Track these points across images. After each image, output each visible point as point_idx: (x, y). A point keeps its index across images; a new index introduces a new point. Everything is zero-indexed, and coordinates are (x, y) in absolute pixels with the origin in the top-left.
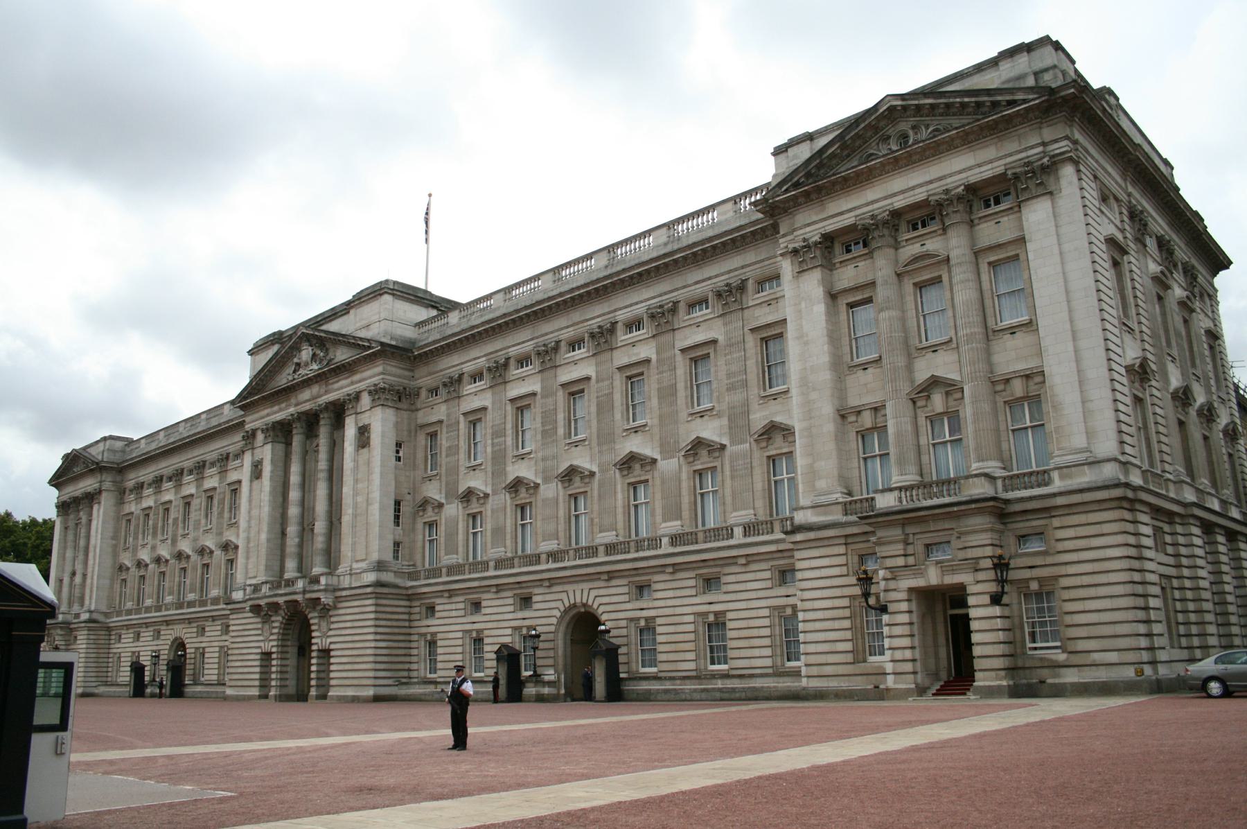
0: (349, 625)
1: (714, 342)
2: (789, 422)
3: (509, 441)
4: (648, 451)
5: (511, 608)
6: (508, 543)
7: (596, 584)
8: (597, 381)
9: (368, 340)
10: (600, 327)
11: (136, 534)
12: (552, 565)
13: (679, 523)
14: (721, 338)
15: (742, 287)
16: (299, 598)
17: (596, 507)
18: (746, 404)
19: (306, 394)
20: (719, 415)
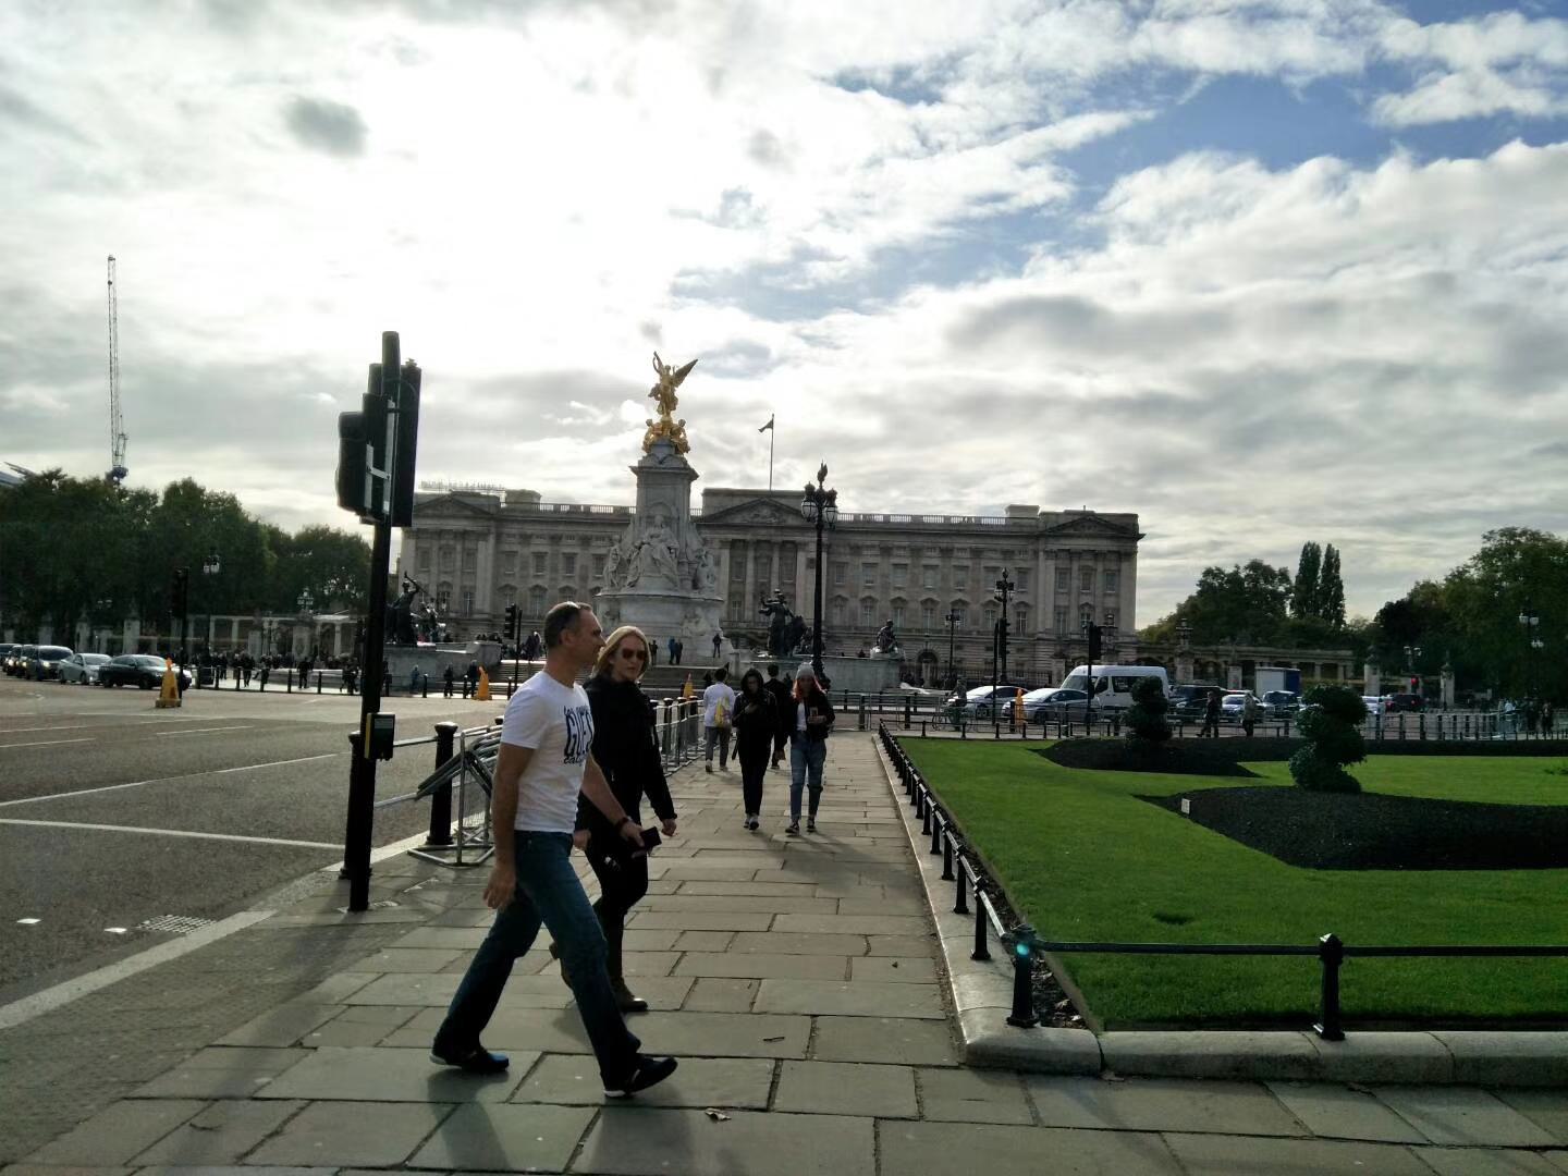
4: (966, 598)
11: (524, 567)
15: (1013, 552)
19: (764, 532)
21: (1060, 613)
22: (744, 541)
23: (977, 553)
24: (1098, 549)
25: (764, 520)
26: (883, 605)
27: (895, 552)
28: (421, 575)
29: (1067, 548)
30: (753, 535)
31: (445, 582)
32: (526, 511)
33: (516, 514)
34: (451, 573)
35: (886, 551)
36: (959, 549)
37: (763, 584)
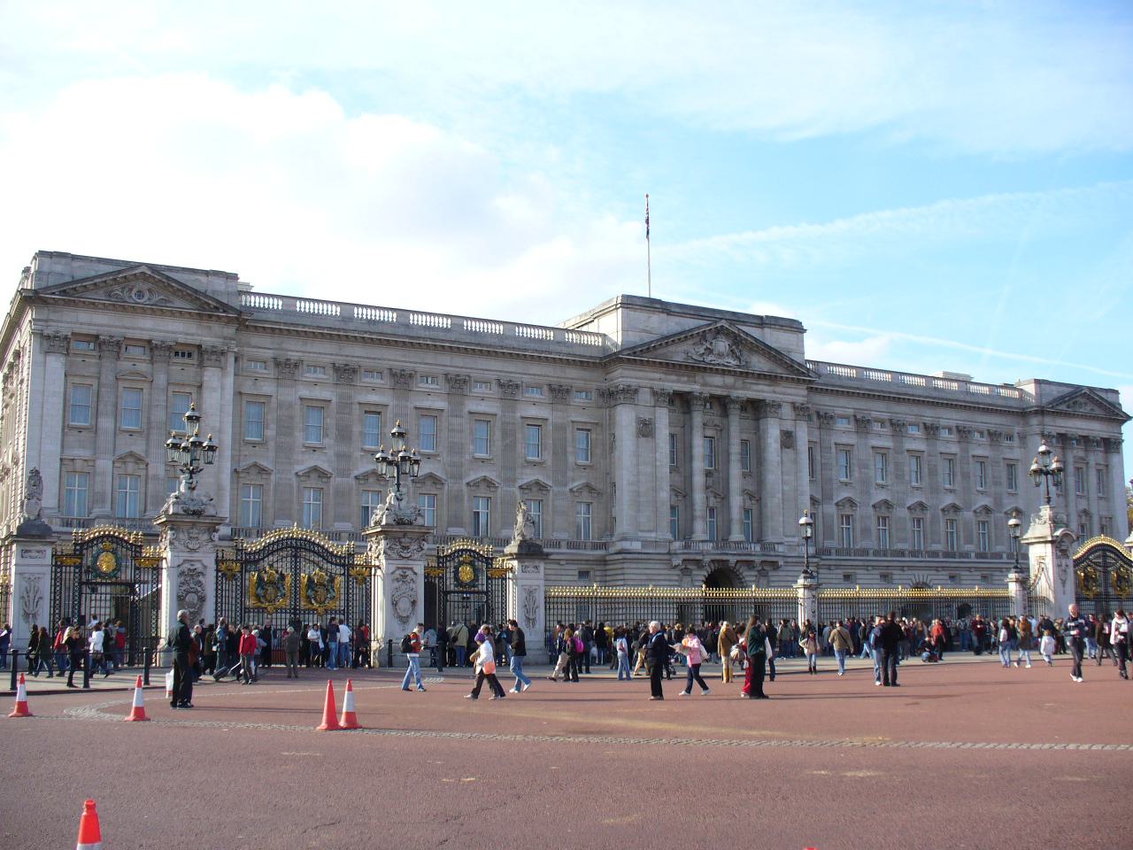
1: (987, 457)
5: (878, 581)
6: (874, 539)
8: (929, 455)
11: (285, 428)
12: (911, 559)
15: (1000, 434)
19: (717, 380)
23: (963, 433)
24: (1092, 434)
25: (720, 361)
26: (865, 514)
27: (877, 427)
28: (73, 437)
29: (1062, 431)
30: (705, 385)
31: (131, 454)
32: (284, 312)
33: (272, 317)
34: (145, 433)
35: (862, 424)
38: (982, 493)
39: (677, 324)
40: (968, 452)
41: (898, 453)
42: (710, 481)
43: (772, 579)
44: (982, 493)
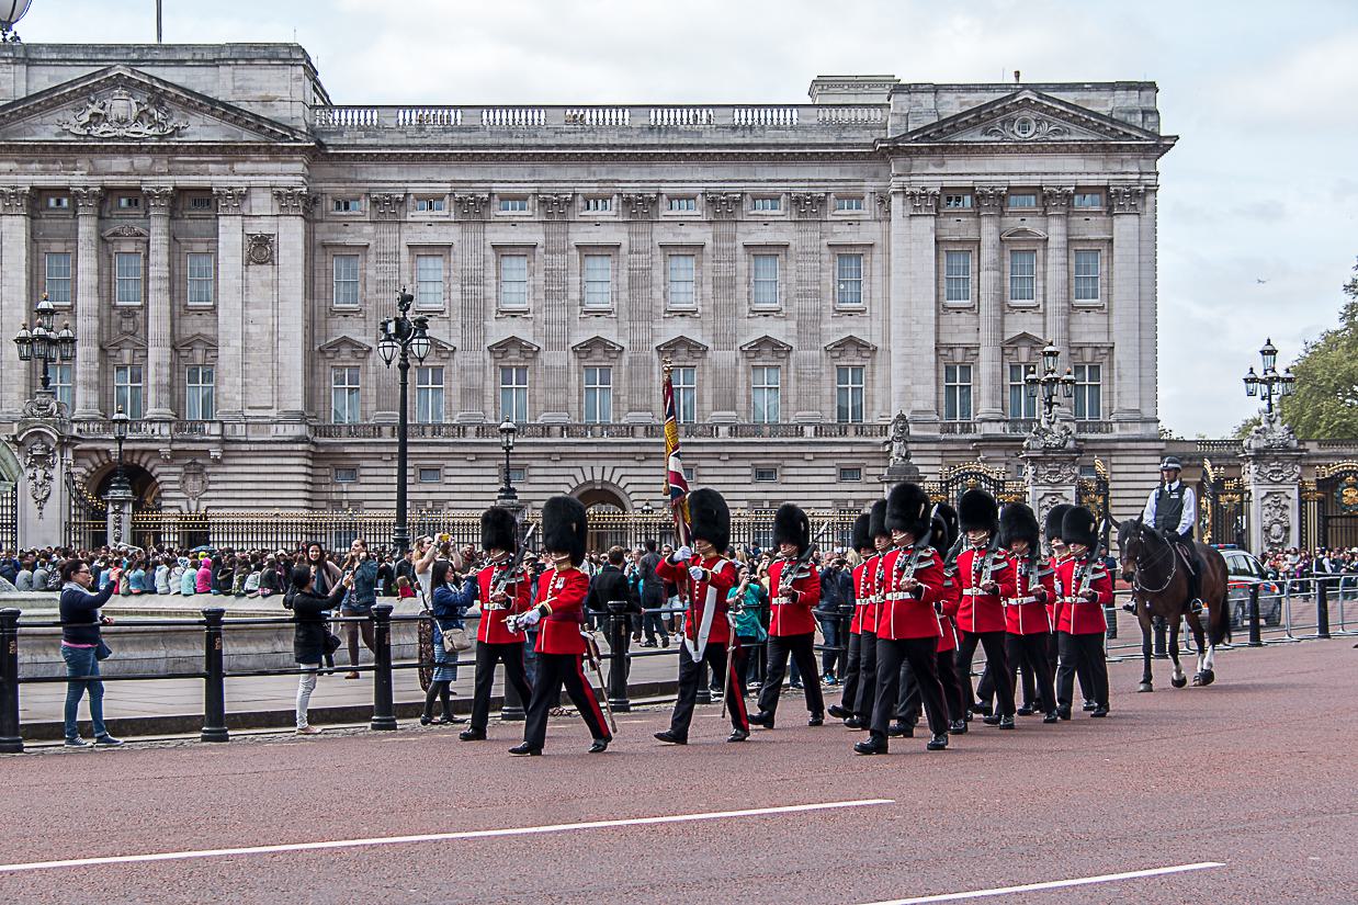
0: (250, 486)
2: (867, 339)
3: (491, 292)
4: (696, 336)
6: (489, 407)
7: (623, 463)
8: (630, 252)
9: (290, 129)
10: (641, 195)
12: (565, 439)
13: (734, 413)
14: (792, 243)
15: (822, 202)
16: (164, 448)
17: (624, 384)
18: (819, 313)
19: (120, 163)
20: (784, 318)
21: (954, 369)
22: (64, 191)
23: (723, 207)
24: (1048, 181)
25: (122, 132)
29: (967, 182)
35: (473, 209)
36: (671, 199)
37: (129, 313)
38: (766, 314)
39: (51, 78)
40: (734, 239)
41: (552, 253)
42: (128, 326)
43: (211, 478)
44: (766, 314)
